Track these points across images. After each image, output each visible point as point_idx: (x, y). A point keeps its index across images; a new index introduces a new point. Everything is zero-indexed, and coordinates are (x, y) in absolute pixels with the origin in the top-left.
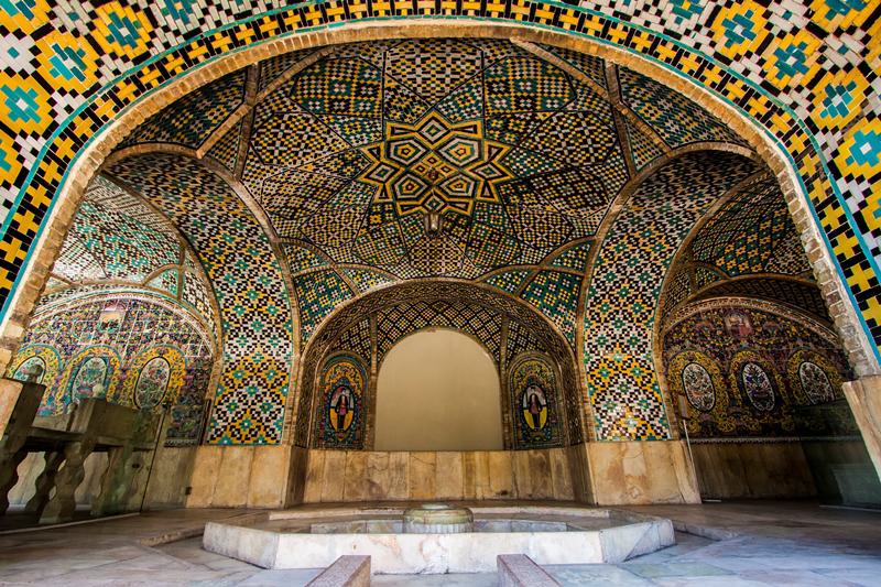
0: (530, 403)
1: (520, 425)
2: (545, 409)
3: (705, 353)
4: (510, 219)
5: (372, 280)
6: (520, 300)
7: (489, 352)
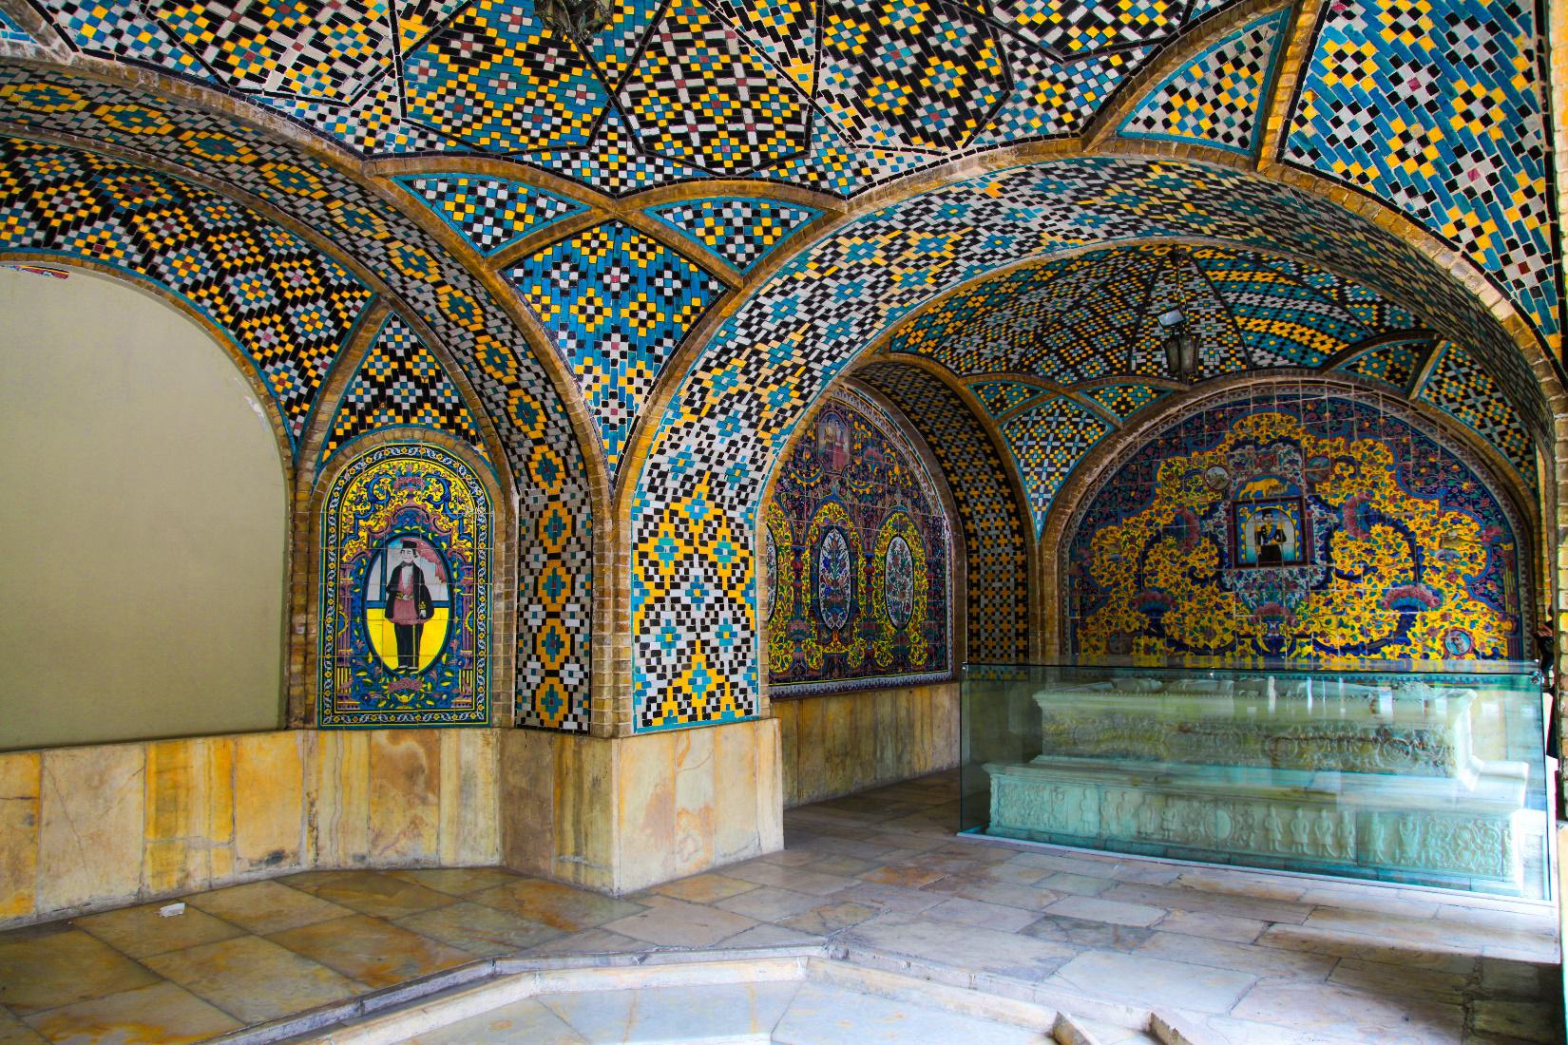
0: (391, 588)
1: (347, 651)
2: (442, 615)
4: (653, 30)
6: (498, 283)
7: (270, 398)
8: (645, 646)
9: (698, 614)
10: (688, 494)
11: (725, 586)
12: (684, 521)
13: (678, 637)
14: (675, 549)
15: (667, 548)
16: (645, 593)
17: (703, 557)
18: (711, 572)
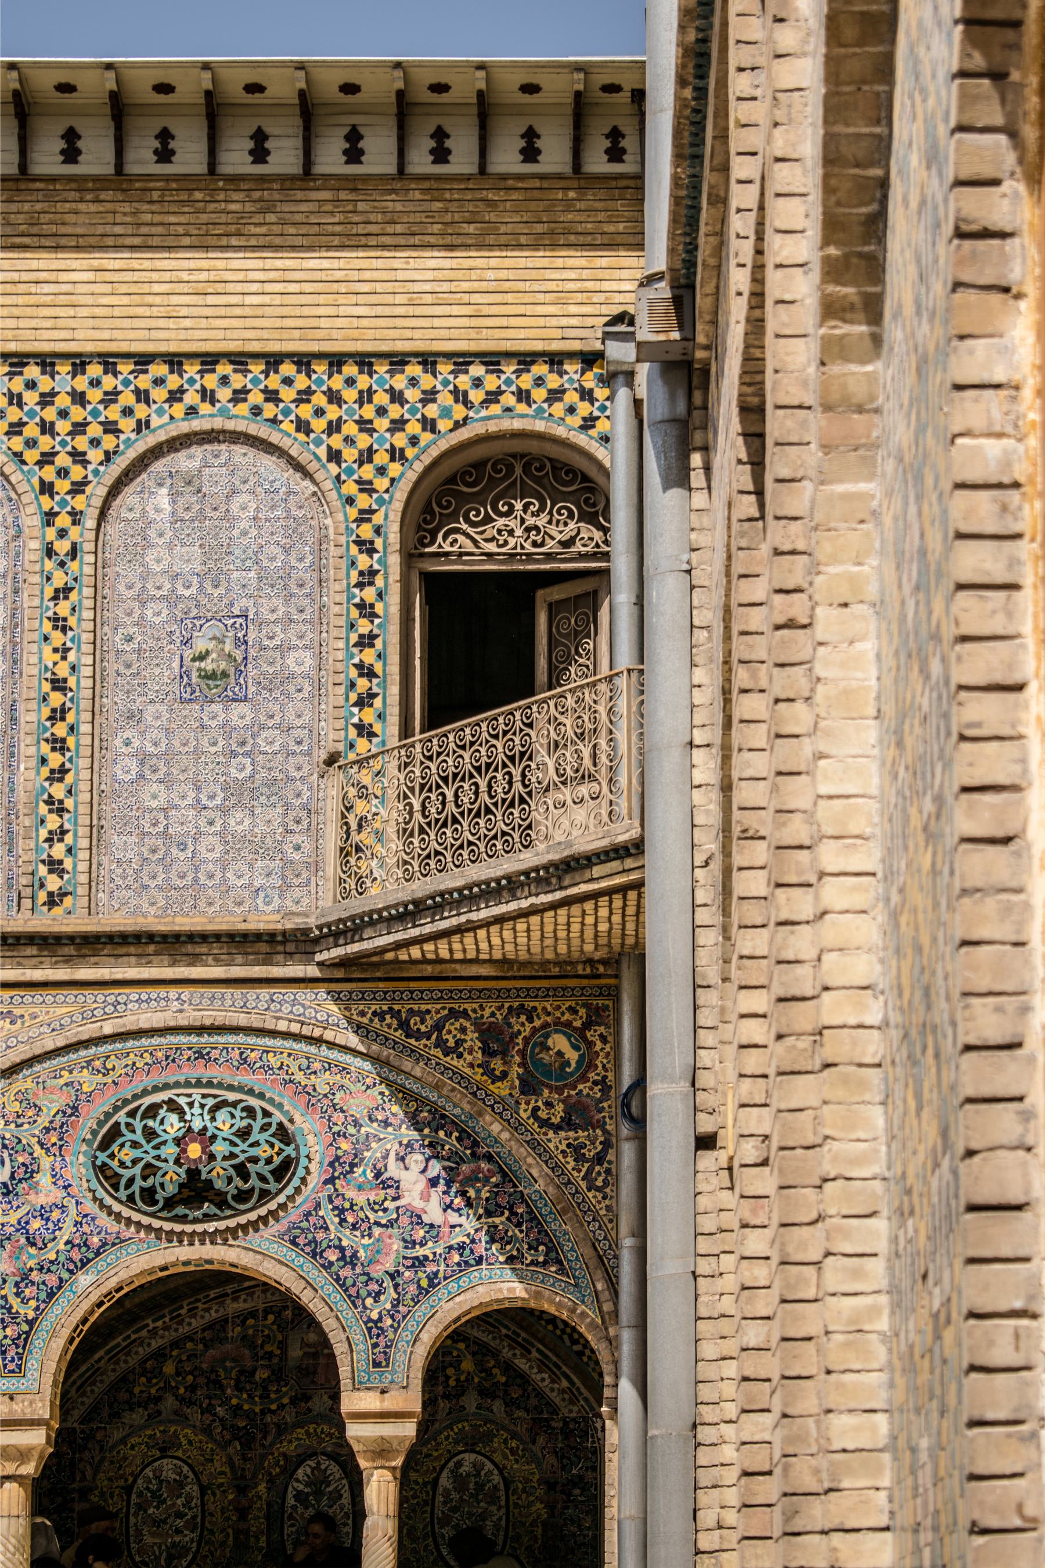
3: (207, 1431)
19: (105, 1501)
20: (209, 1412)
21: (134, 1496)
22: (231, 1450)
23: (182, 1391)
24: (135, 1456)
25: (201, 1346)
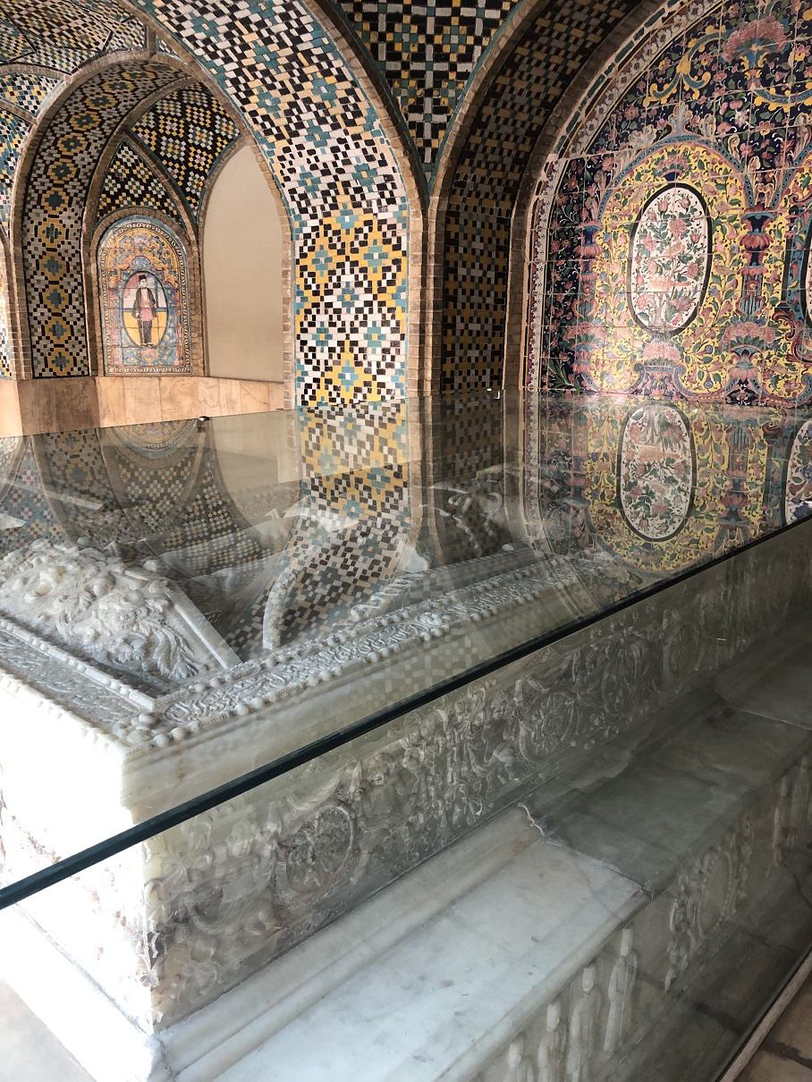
3: (722, 146)
5: (37, 88)
8: (304, 343)
9: (348, 317)
10: (334, 206)
11: (375, 291)
12: (337, 233)
13: (330, 337)
14: (329, 260)
15: (322, 260)
16: (304, 299)
17: (355, 263)
18: (361, 278)
19: (609, 244)
20: (726, 119)
21: (637, 236)
22: (748, 170)
23: (696, 96)
24: (640, 188)
25: (723, 29)
